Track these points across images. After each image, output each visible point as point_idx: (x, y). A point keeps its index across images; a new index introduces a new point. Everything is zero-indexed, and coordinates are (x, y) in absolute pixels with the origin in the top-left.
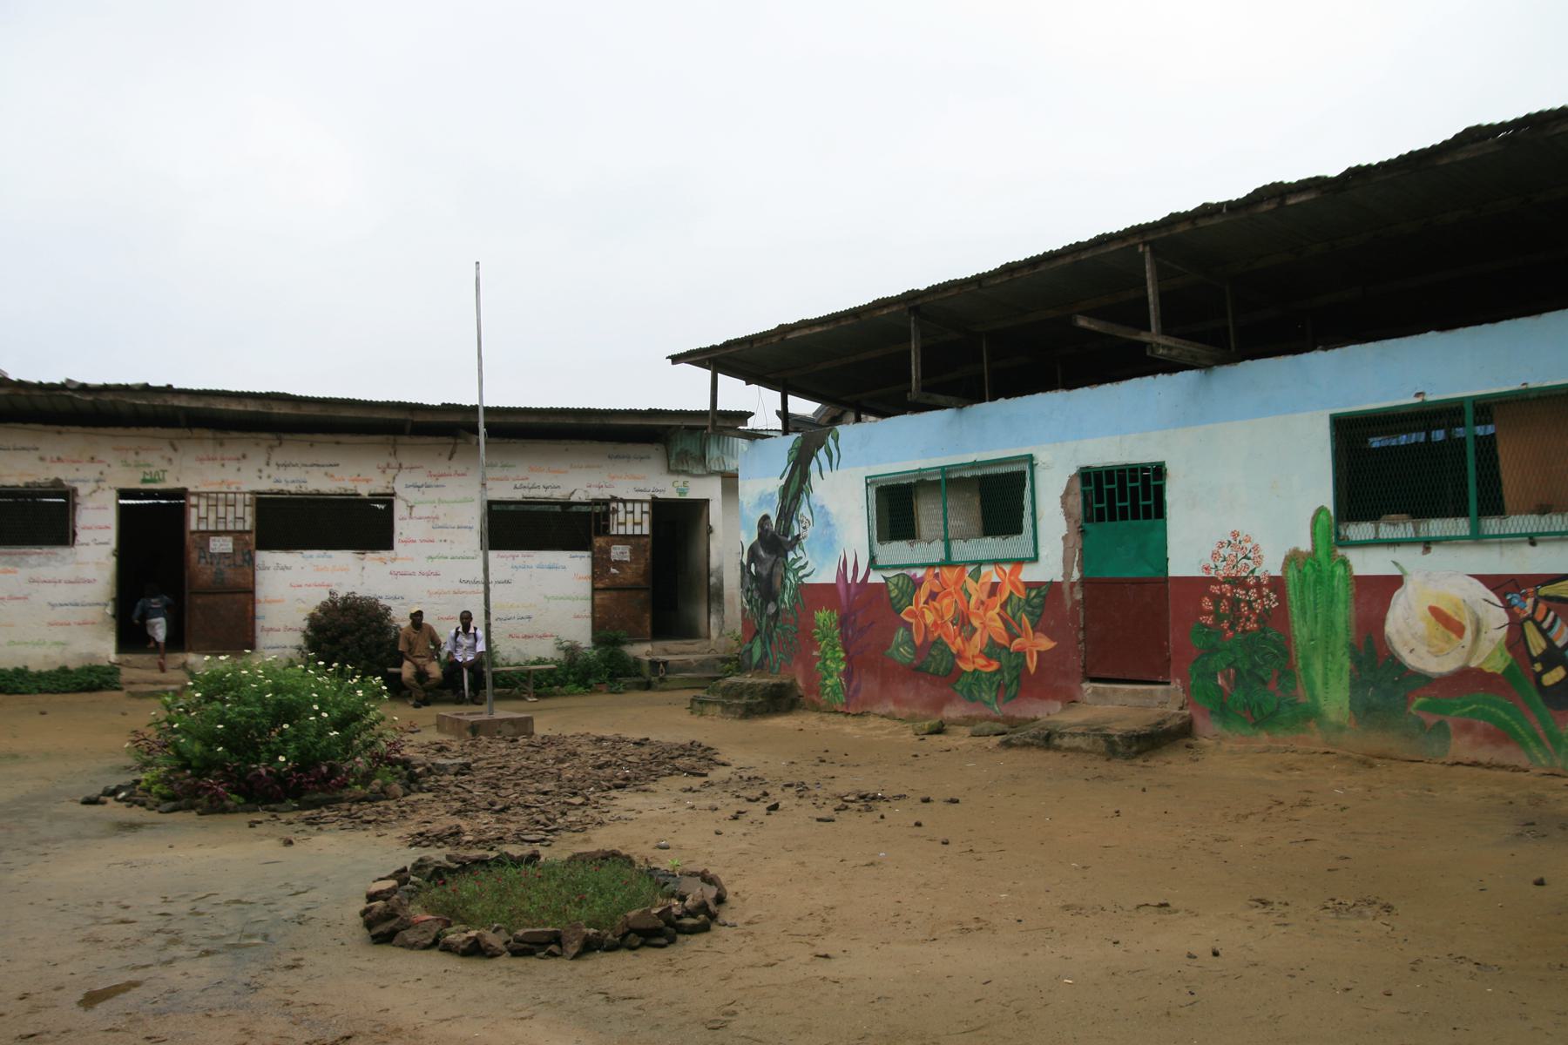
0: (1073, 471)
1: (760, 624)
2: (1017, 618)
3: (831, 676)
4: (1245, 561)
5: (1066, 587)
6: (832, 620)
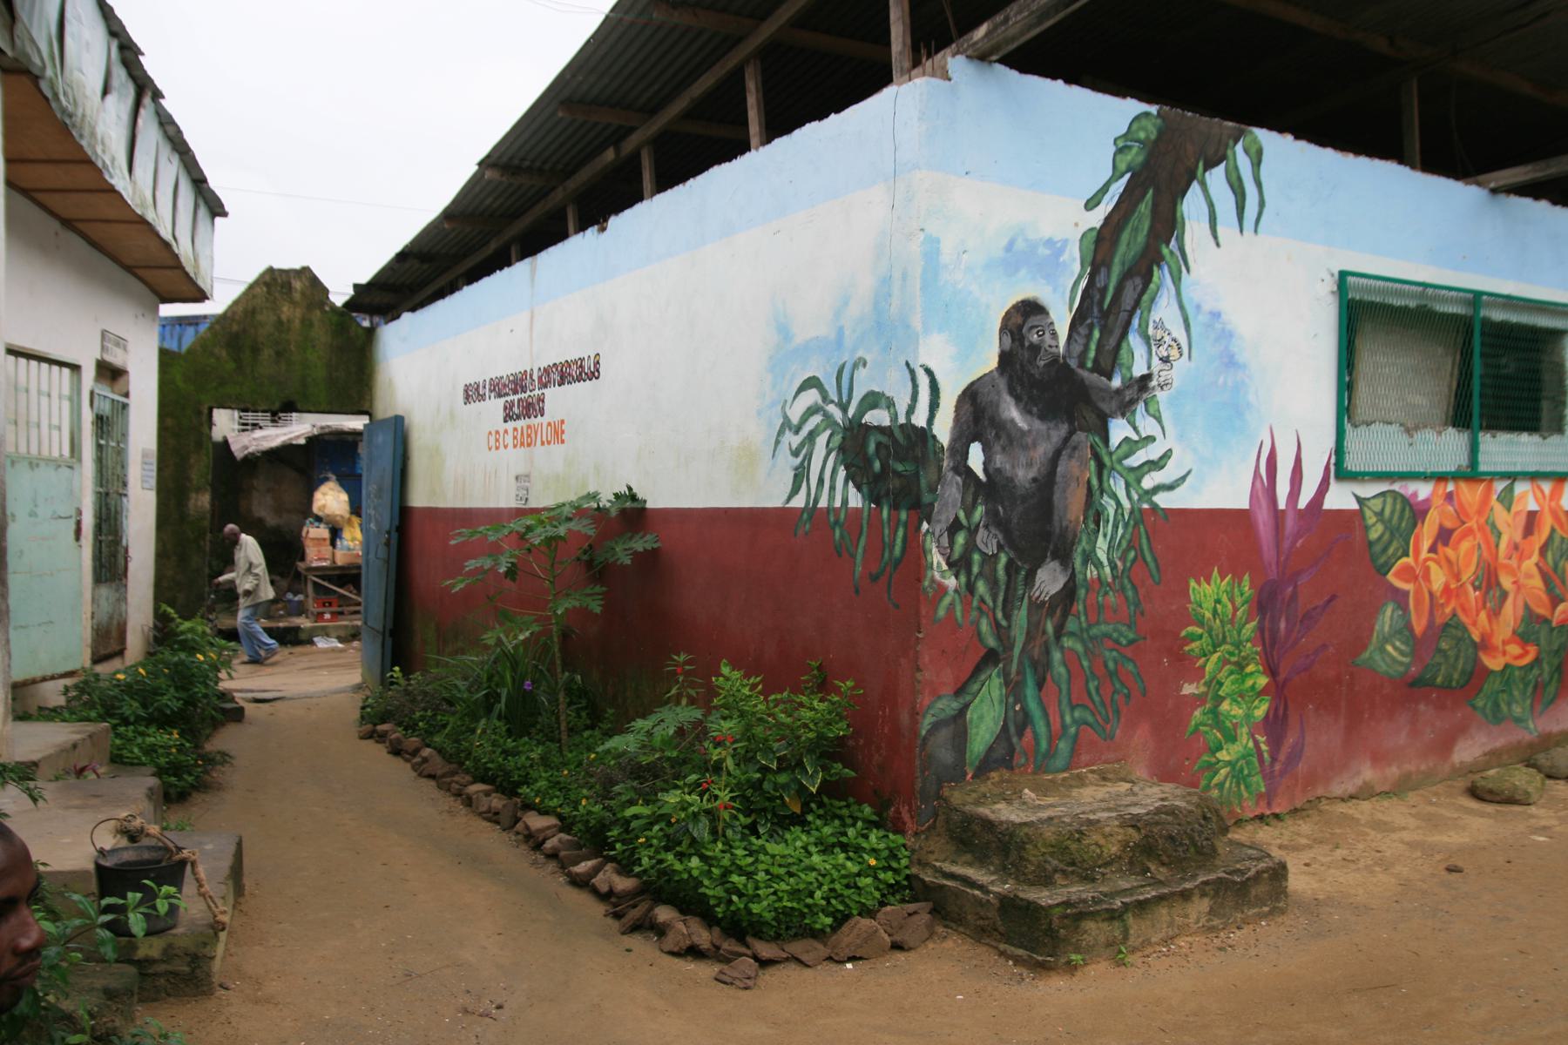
1: (1001, 632)
3: (1232, 738)
6: (1238, 600)
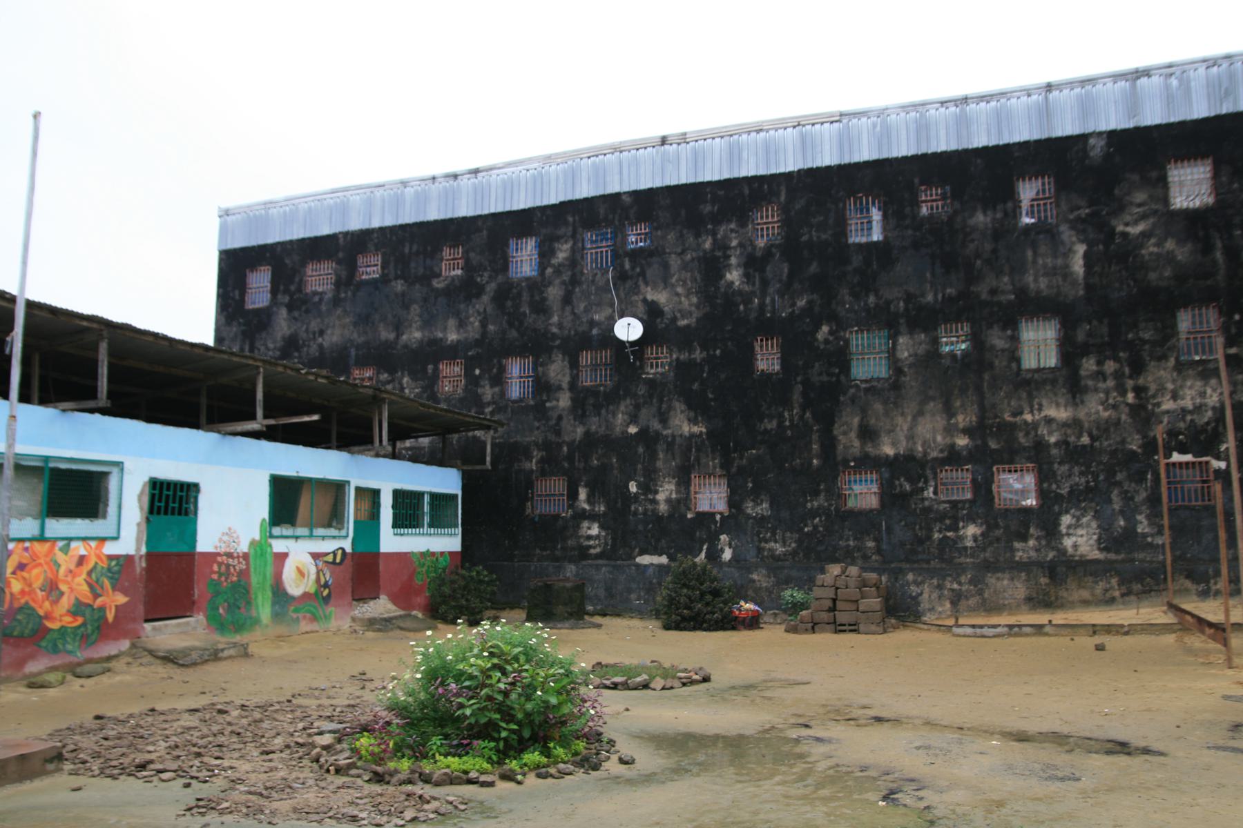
0: (146, 479)
5: (137, 559)
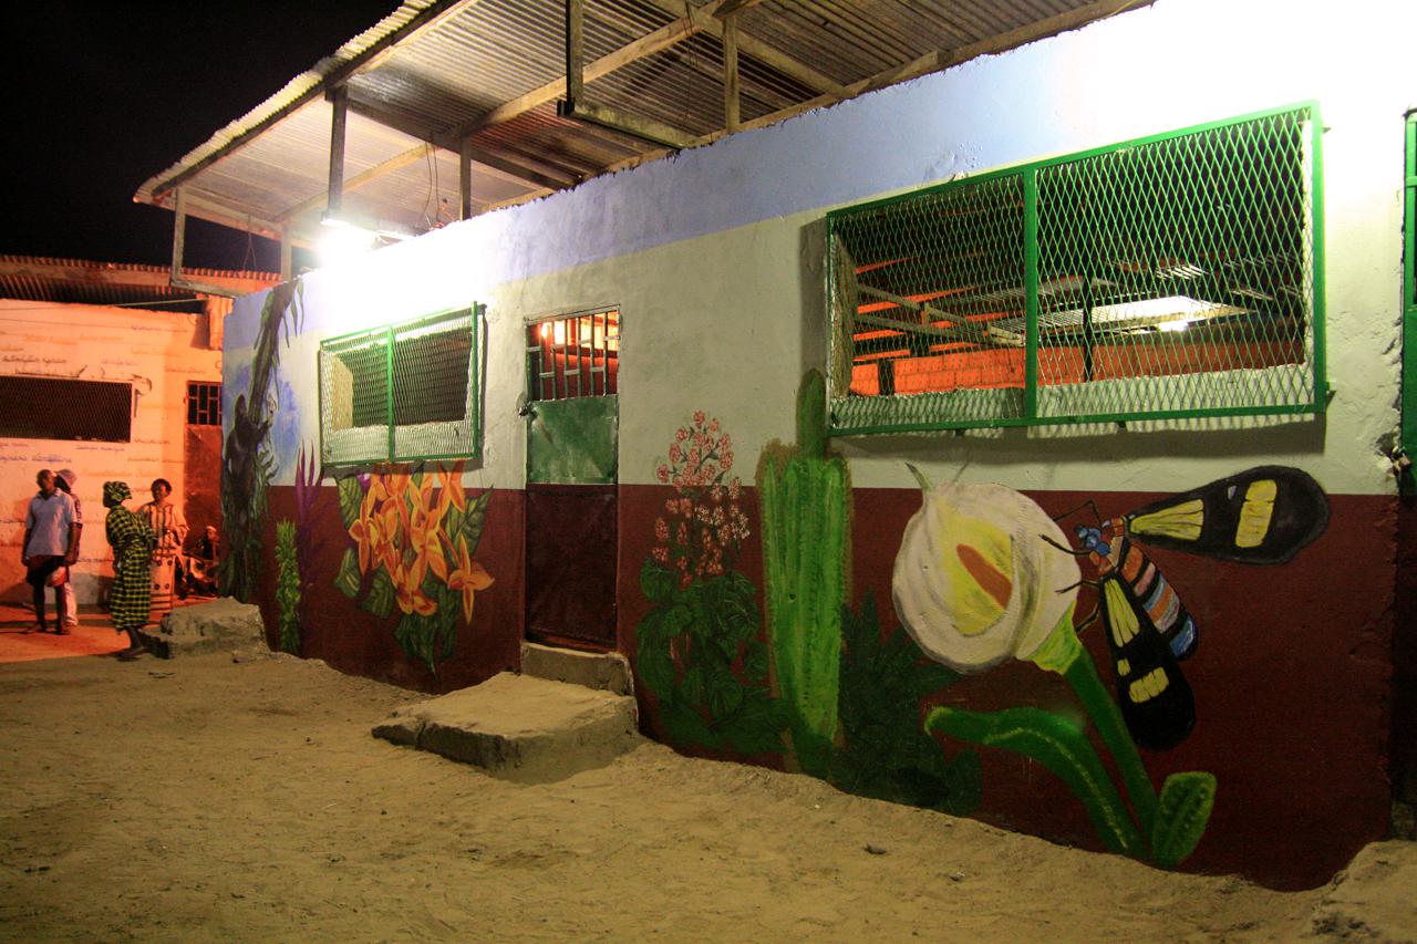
2: (456, 541)
4: (709, 461)
